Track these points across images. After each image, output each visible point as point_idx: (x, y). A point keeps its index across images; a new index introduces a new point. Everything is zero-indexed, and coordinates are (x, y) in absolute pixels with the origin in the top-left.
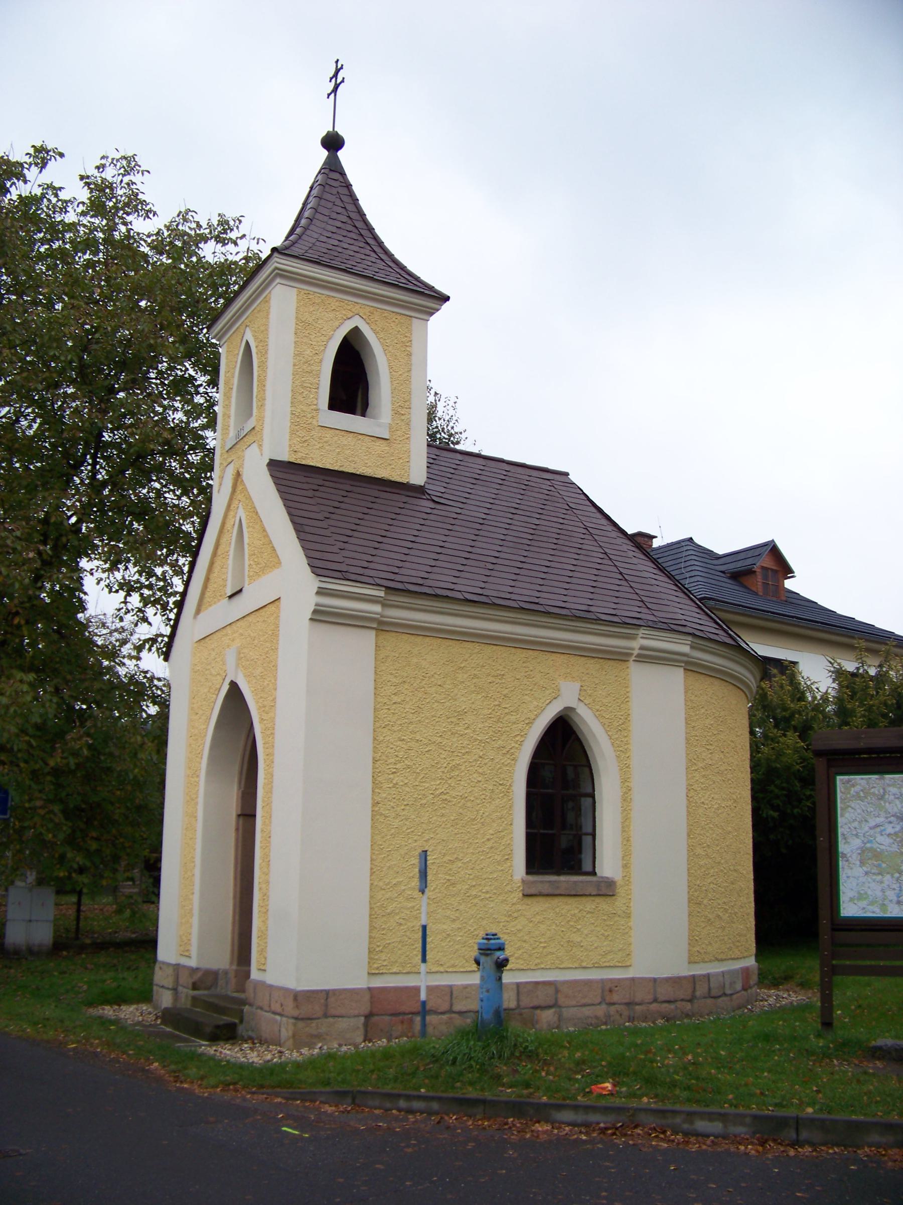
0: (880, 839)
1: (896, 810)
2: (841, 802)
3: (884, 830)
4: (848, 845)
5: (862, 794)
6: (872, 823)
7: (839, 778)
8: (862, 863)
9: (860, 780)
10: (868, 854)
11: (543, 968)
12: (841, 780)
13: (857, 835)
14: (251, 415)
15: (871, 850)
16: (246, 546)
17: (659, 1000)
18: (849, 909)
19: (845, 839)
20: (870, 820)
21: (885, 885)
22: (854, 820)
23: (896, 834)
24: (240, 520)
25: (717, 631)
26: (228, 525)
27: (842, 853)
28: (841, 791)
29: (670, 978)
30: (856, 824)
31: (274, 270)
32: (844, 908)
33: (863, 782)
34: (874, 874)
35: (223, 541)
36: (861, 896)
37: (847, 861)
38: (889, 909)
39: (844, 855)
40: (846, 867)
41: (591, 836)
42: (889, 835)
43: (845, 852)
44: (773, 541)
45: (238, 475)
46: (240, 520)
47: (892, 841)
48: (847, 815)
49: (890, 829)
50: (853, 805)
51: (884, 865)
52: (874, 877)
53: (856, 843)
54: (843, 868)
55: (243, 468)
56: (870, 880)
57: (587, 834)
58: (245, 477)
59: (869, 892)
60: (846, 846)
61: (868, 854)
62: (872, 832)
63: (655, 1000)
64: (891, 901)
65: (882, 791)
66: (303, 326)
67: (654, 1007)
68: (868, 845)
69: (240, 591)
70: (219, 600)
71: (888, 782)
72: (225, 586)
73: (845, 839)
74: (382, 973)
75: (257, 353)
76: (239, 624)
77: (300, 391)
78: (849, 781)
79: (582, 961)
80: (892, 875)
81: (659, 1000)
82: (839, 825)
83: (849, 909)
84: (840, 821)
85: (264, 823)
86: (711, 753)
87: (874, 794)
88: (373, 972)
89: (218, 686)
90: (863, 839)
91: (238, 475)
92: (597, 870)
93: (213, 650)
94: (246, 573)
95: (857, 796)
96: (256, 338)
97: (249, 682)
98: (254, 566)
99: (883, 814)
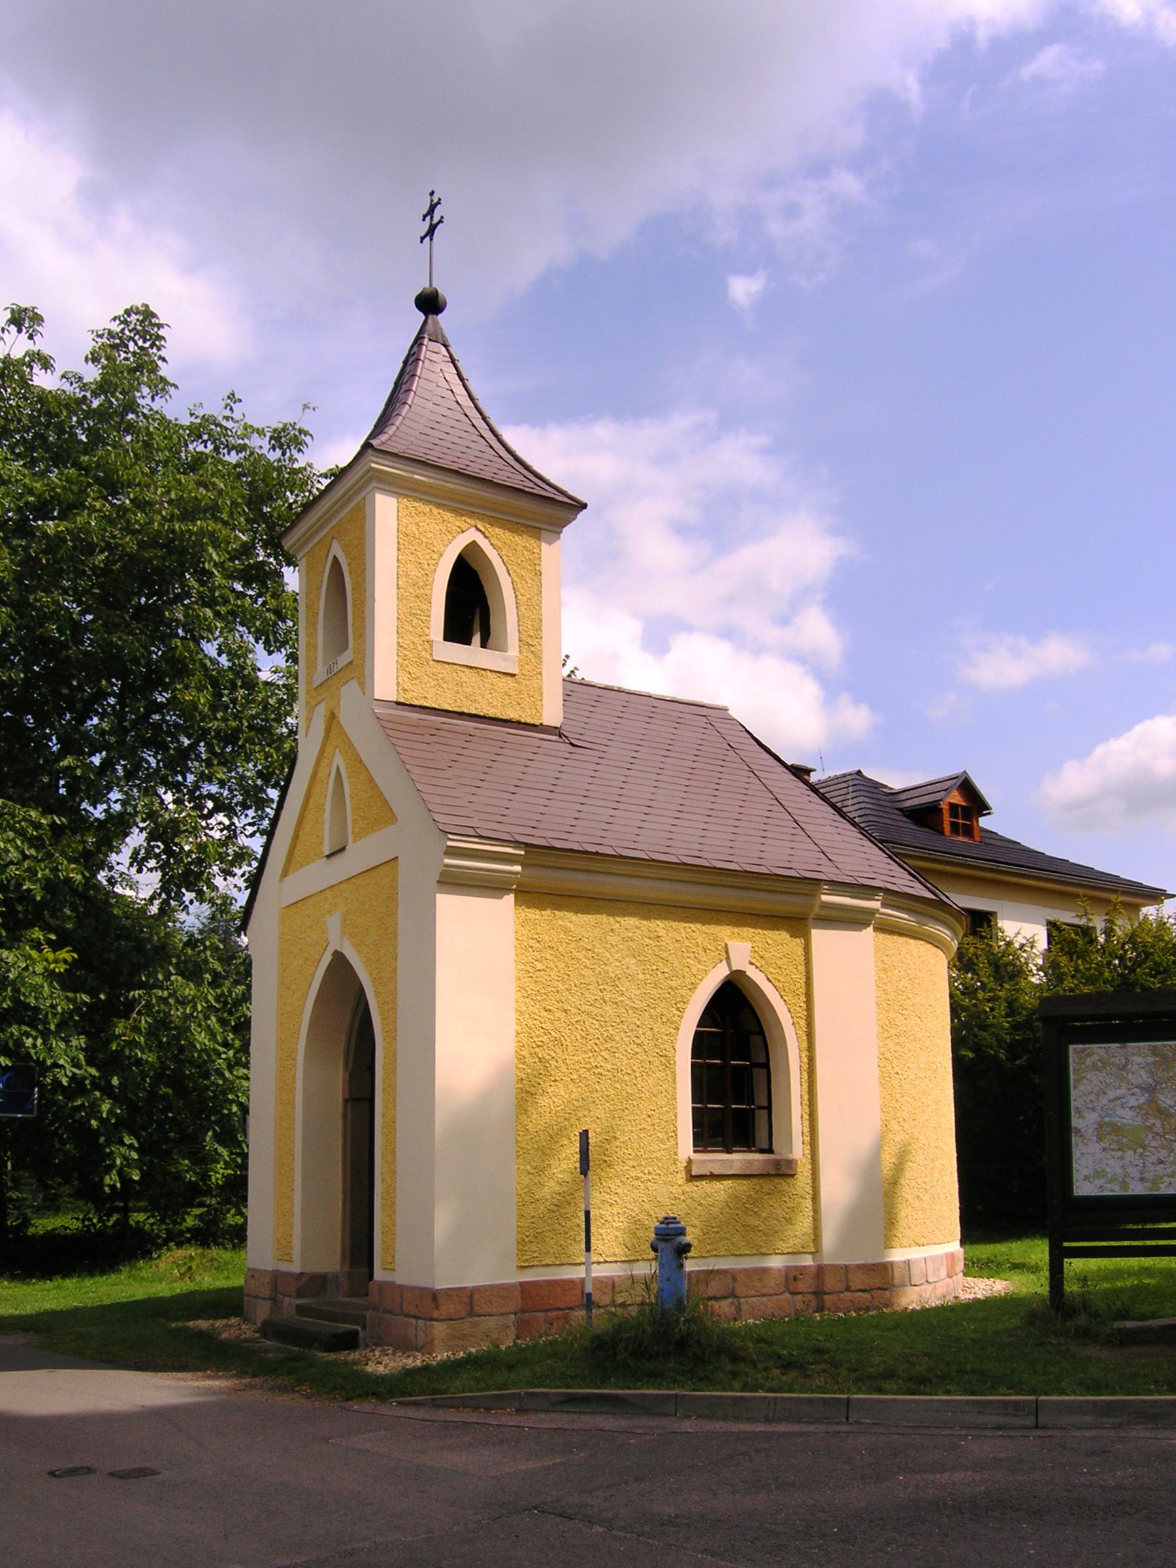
0: (1120, 1112)
1: (1140, 1080)
2: (1074, 1074)
3: (1127, 1102)
4: (1083, 1121)
5: (1099, 1064)
6: (1112, 1094)
7: (1071, 1047)
8: (1099, 1139)
9: (1098, 1050)
10: (1108, 1130)
11: (716, 1256)
12: (1075, 1050)
13: (1093, 1109)
14: (346, 647)
15: (1109, 1124)
16: (348, 799)
17: (853, 1288)
18: (1083, 1187)
19: (1079, 1113)
20: (1109, 1092)
21: (1126, 1161)
22: (1090, 1093)
23: (1140, 1107)
24: (338, 768)
25: (912, 884)
26: (322, 772)
27: (1076, 1128)
28: (1074, 1062)
29: (864, 1265)
30: (1092, 1097)
31: (368, 471)
32: (1077, 1187)
33: (1102, 1052)
34: (1113, 1150)
35: (317, 790)
36: (1097, 1174)
37: (1082, 1136)
38: (1131, 1186)
39: (1078, 1131)
40: (1080, 1143)
41: (766, 1111)
42: (1131, 1108)
43: (1079, 1127)
44: (965, 772)
45: (332, 717)
46: (338, 768)
47: (1134, 1114)
48: (1081, 1087)
49: (1132, 1101)
50: (1088, 1077)
51: (1125, 1140)
52: (1113, 1153)
53: (1093, 1117)
54: (1077, 1144)
55: (339, 709)
56: (1108, 1156)
57: (760, 1108)
58: (343, 719)
59: (1108, 1169)
60: (1080, 1120)
61: (1108, 1130)
62: (1111, 1105)
63: (848, 1289)
64: (1133, 1178)
65: (1123, 1061)
66: (405, 540)
67: (847, 1295)
68: (1107, 1119)
69: (343, 849)
70: (314, 860)
71: (1131, 1050)
72: (321, 844)
73: (1079, 1113)
74: (533, 1266)
75: (350, 573)
76: (342, 887)
77: (409, 618)
78: (1083, 1051)
79: (761, 1247)
80: (1135, 1151)
81: (853, 1288)
82: (1072, 1098)
83: (1083, 1187)
84: (1073, 1093)
85: (385, 1107)
86: (906, 1019)
87: (1114, 1064)
88: (523, 1264)
89: (317, 957)
90: (1100, 1112)
91: (332, 717)
92: (774, 1147)
93: (309, 916)
94: (350, 829)
95: (1095, 1067)
96: (347, 553)
97: (359, 952)
98: (361, 822)
99: (1124, 1086)
